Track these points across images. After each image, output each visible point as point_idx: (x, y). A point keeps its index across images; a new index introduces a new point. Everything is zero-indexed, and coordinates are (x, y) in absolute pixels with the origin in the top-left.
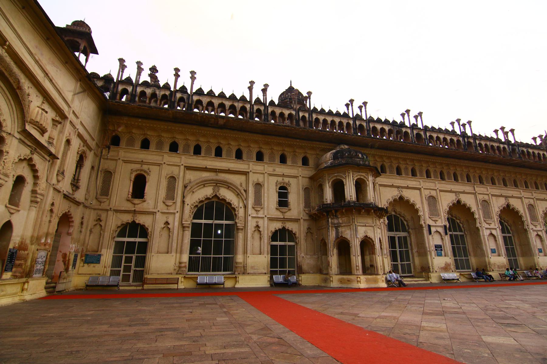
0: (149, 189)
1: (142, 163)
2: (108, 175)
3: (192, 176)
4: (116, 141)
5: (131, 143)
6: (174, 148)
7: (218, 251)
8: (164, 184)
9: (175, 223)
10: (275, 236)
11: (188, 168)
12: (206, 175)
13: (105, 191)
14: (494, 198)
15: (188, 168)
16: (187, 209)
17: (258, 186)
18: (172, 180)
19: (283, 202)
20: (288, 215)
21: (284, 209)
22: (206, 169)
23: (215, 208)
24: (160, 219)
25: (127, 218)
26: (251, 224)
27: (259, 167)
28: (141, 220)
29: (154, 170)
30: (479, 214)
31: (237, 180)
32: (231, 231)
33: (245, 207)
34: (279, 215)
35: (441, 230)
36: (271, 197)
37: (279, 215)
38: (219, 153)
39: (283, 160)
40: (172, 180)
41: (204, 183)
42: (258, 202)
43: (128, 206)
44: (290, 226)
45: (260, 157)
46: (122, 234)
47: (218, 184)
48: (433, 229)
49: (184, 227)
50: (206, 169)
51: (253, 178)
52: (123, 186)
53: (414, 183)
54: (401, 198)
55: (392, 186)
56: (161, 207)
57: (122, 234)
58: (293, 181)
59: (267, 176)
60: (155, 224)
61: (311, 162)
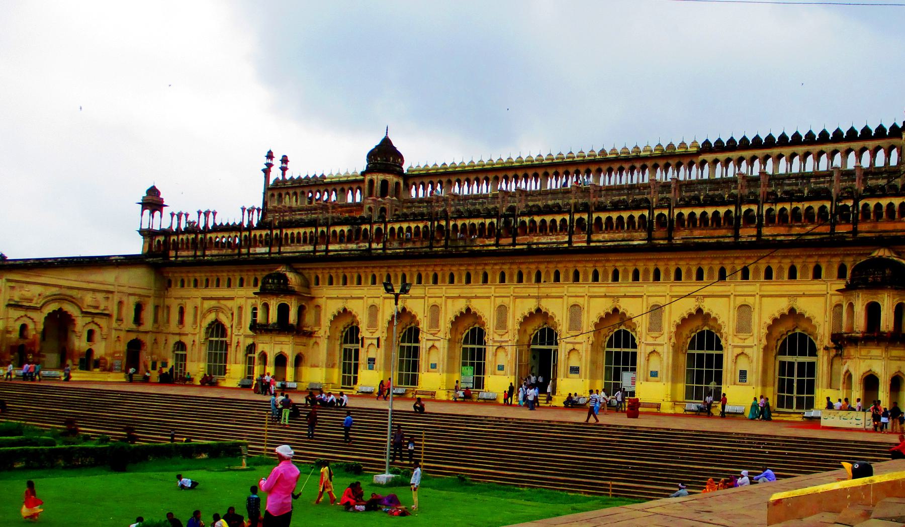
1: (181, 298)
4: (169, 284)
9: (197, 342)
11: (204, 299)
12: (213, 303)
15: (204, 299)
16: (203, 330)
17: (240, 308)
22: (211, 299)
23: (217, 328)
25: (177, 338)
31: (229, 303)
33: (232, 326)
35: (375, 342)
41: (210, 311)
42: (240, 323)
47: (217, 309)
48: (367, 342)
50: (211, 299)
53: (360, 292)
60: (187, 340)
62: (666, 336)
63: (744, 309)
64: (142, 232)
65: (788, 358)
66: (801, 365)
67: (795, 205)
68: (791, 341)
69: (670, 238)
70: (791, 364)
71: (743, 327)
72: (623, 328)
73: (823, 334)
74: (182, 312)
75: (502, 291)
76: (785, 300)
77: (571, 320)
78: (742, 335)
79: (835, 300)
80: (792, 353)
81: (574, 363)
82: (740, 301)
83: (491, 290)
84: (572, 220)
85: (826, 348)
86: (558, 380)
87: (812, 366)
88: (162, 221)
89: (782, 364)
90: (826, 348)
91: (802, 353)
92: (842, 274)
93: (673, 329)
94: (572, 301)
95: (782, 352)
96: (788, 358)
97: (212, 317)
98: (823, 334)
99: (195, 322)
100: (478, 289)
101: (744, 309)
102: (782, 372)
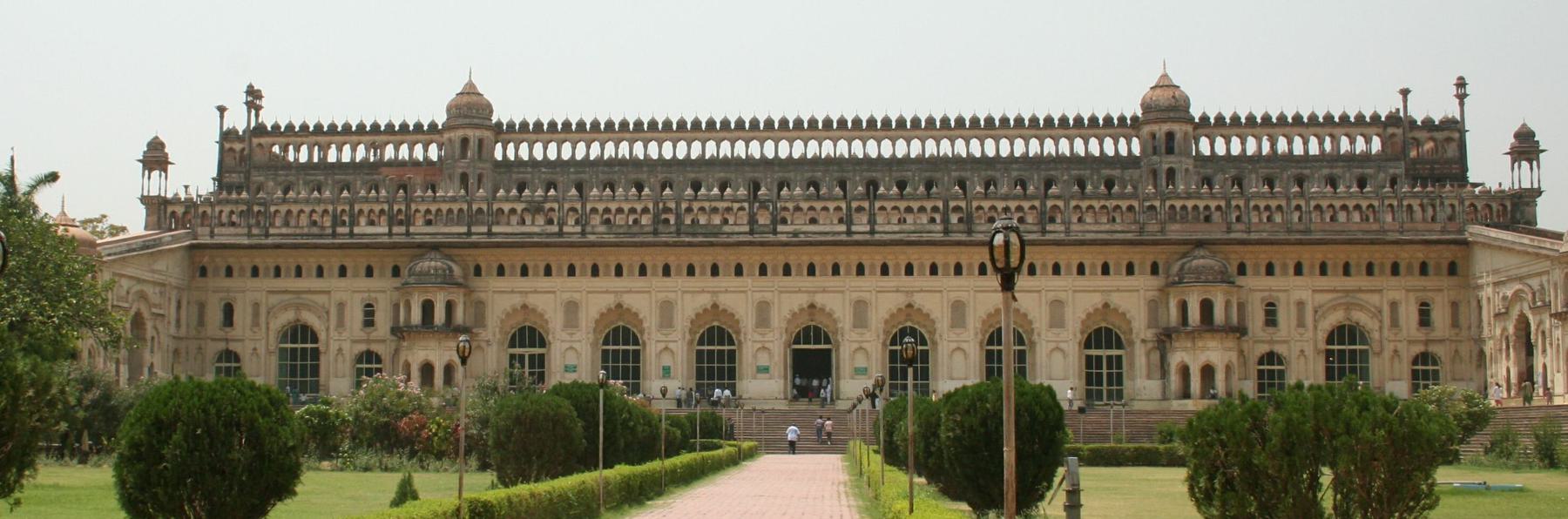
0: (237, 317)
1: (228, 291)
2: (202, 307)
3: (274, 299)
5: (216, 274)
6: (255, 272)
7: (304, 375)
8: (249, 310)
10: (359, 359)
13: (201, 322)
14: (688, 297)
18: (256, 306)
19: (369, 322)
20: (374, 335)
21: (369, 329)
23: (301, 332)
24: (249, 345)
25: (222, 346)
26: (334, 347)
27: (343, 282)
28: (233, 346)
29: (239, 296)
30: (650, 320)
32: (316, 354)
33: (328, 329)
34: (362, 335)
36: (356, 315)
37: (362, 335)
38: (299, 273)
39: (369, 272)
40: (256, 306)
41: (286, 308)
42: (341, 323)
43: (221, 334)
44: (375, 348)
45: (343, 272)
46: (220, 360)
47: (298, 307)
49: (269, 353)
51: (337, 297)
52: (215, 315)
54: (525, 307)
55: (512, 292)
56: (248, 333)
57: (220, 360)
58: (379, 296)
59: (351, 292)
61: (404, 272)
62: (972, 332)
63: (1057, 305)
64: (145, 200)
65: (1094, 352)
66: (1109, 358)
67: (1103, 203)
68: (1102, 338)
69: (970, 232)
70: (1099, 358)
71: (1057, 322)
72: (909, 324)
73: (1140, 328)
74: (229, 311)
75: (763, 281)
76: (1098, 294)
77: (855, 315)
78: (1055, 330)
79: (1151, 294)
80: (1098, 347)
81: (861, 362)
82: (1051, 296)
83: (746, 281)
84: (849, 208)
85: (1143, 341)
86: (842, 382)
87: (1119, 358)
88: (156, 185)
89: (1089, 358)
90: (1143, 341)
91: (1109, 347)
92: (1155, 270)
93: (979, 325)
94: (855, 296)
95: (1088, 345)
96: (1094, 352)
97: (289, 316)
98: (1140, 328)
99: (256, 323)
100: (727, 281)
101: (1057, 305)
102: (1089, 366)
